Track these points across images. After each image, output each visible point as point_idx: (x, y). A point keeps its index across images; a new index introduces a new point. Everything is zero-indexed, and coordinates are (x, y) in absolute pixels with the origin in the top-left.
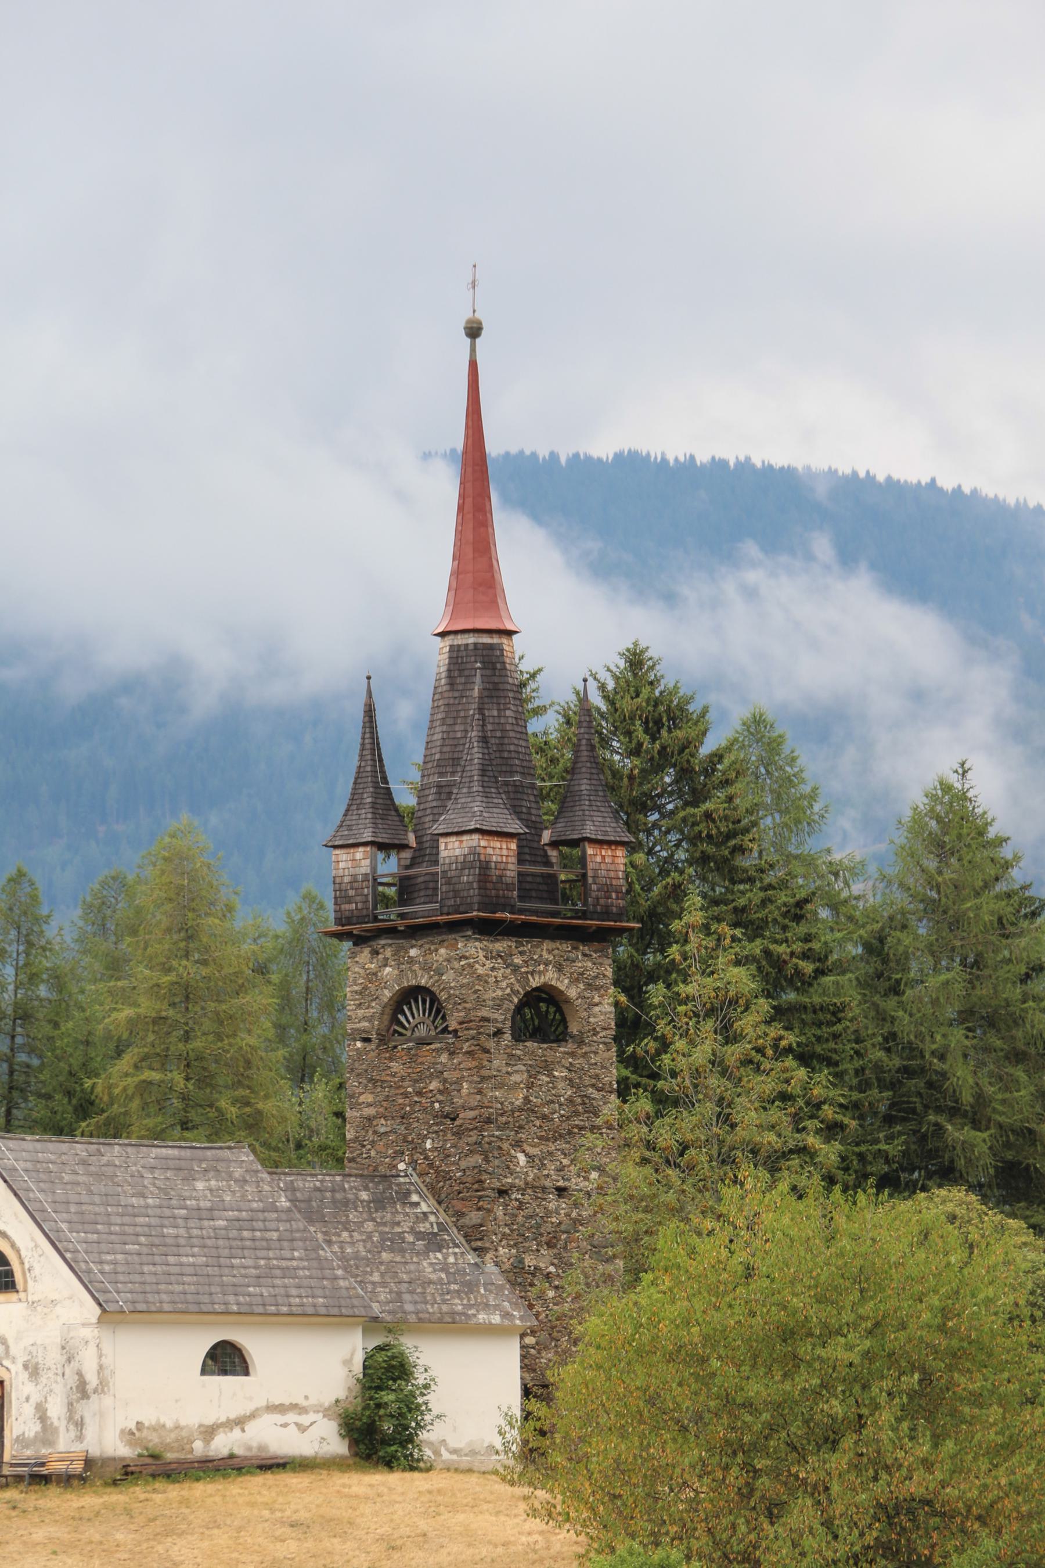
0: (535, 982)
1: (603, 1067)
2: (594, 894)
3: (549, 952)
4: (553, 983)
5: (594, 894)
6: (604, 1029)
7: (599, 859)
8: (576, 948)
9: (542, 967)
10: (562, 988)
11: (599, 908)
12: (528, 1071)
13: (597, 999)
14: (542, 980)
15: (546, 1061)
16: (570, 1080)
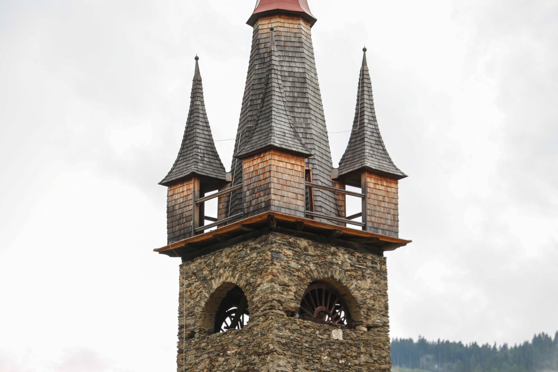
0: (216, 284)
1: (263, 335)
2: (247, 199)
3: (228, 257)
4: (228, 280)
5: (247, 199)
6: (264, 303)
7: (252, 169)
8: (245, 246)
9: (221, 271)
10: (234, 281)
11: (251, 209)
12: (209, 357)
13: (259, 281)
14: (222, 280)
15: (222, 345)
16: (240, 353)
